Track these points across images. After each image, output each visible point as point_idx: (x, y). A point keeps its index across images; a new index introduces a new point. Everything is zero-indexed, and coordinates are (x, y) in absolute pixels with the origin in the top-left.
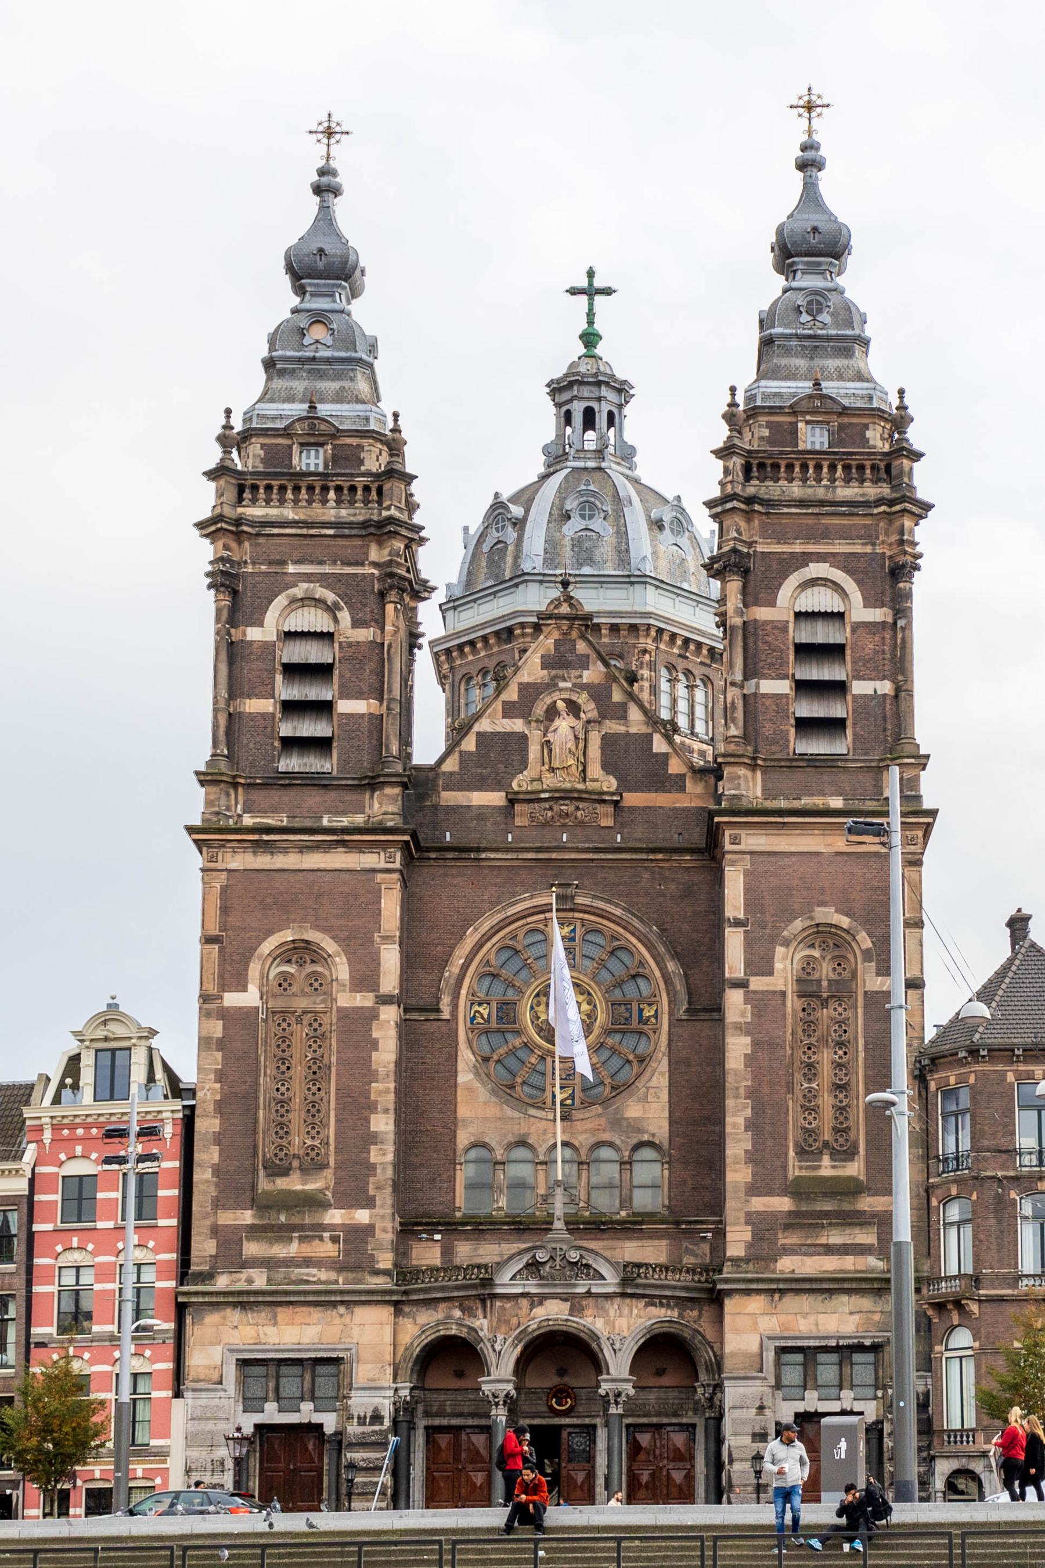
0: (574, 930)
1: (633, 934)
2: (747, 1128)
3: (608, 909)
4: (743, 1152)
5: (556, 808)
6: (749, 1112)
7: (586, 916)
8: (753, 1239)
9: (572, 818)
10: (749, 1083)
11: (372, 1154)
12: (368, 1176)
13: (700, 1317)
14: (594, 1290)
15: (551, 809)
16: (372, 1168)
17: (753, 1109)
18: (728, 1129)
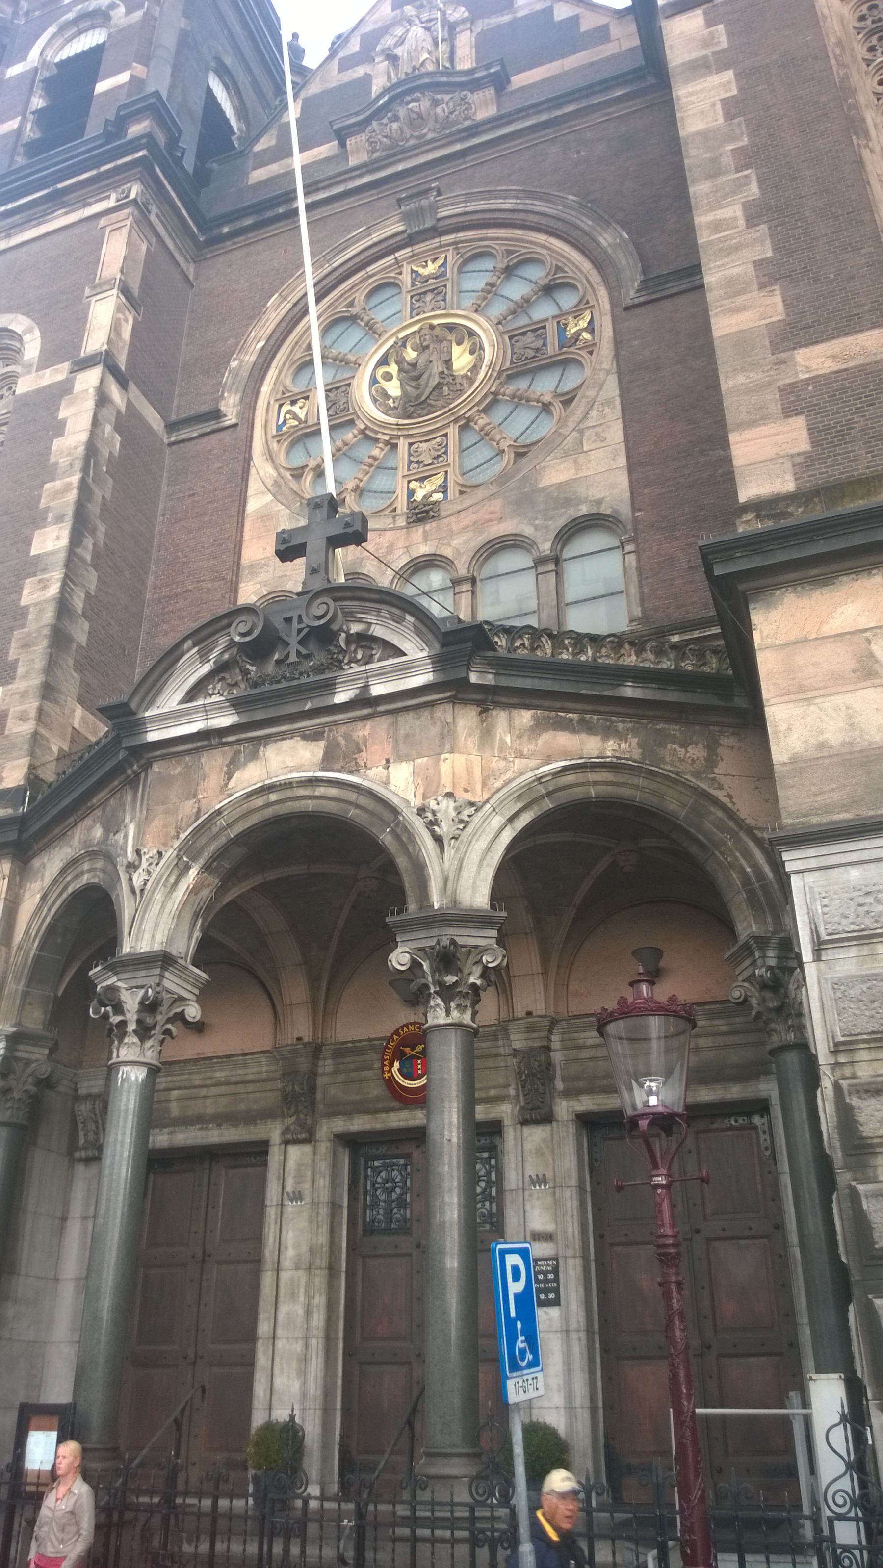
0: (444, 264)
1: (538, 229)
2: (752, 221)
3: (493, 207)
4: (751, 268)
5: (402, 112)
6: (754, 190)
7: (461, 235)
8: (814, 443)
9: (431, 124)
10: (745, 141)
11: (25, 592)
12: (12, 629)
13: (711, 762)
14: (378, 690)
15: (396, 118)
16: (20, 615)
17: (761, 182)
18: (703, 237)
